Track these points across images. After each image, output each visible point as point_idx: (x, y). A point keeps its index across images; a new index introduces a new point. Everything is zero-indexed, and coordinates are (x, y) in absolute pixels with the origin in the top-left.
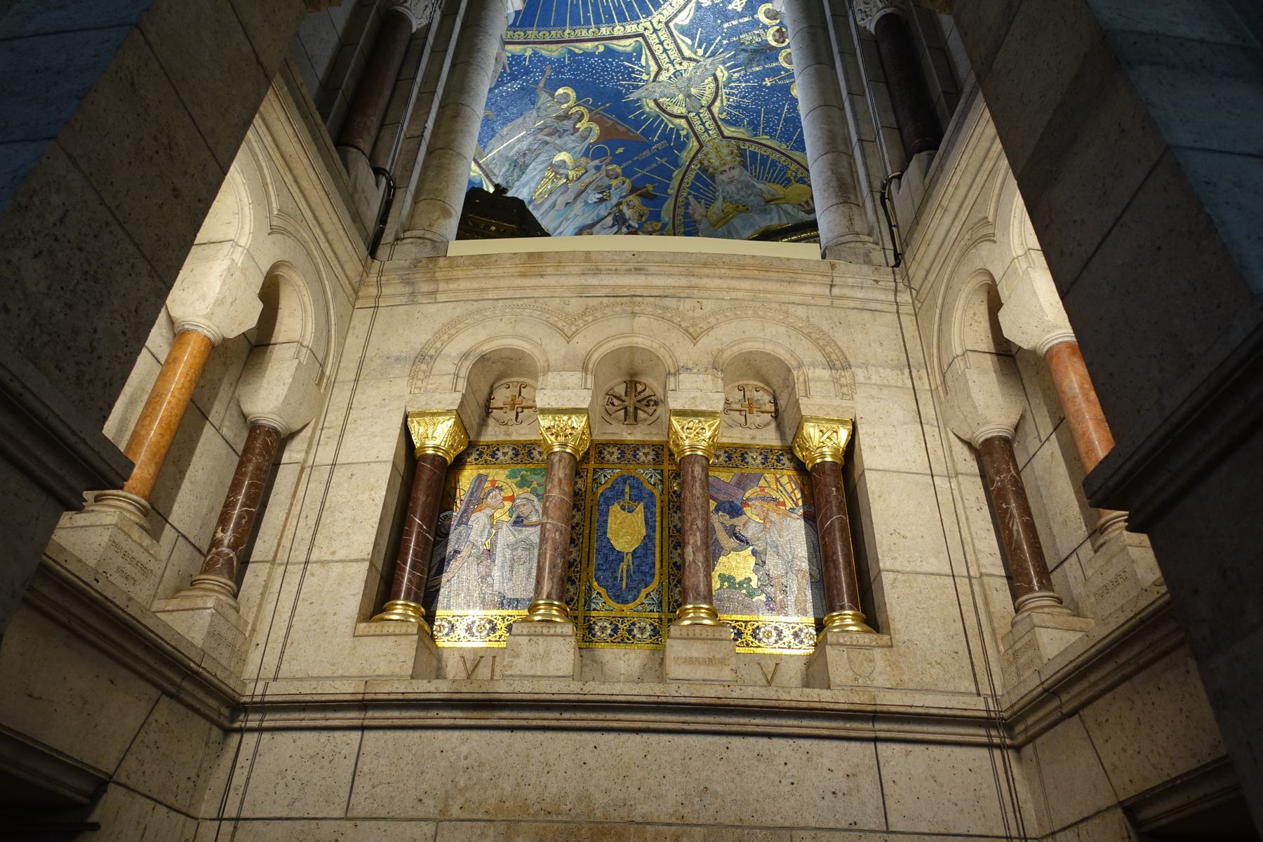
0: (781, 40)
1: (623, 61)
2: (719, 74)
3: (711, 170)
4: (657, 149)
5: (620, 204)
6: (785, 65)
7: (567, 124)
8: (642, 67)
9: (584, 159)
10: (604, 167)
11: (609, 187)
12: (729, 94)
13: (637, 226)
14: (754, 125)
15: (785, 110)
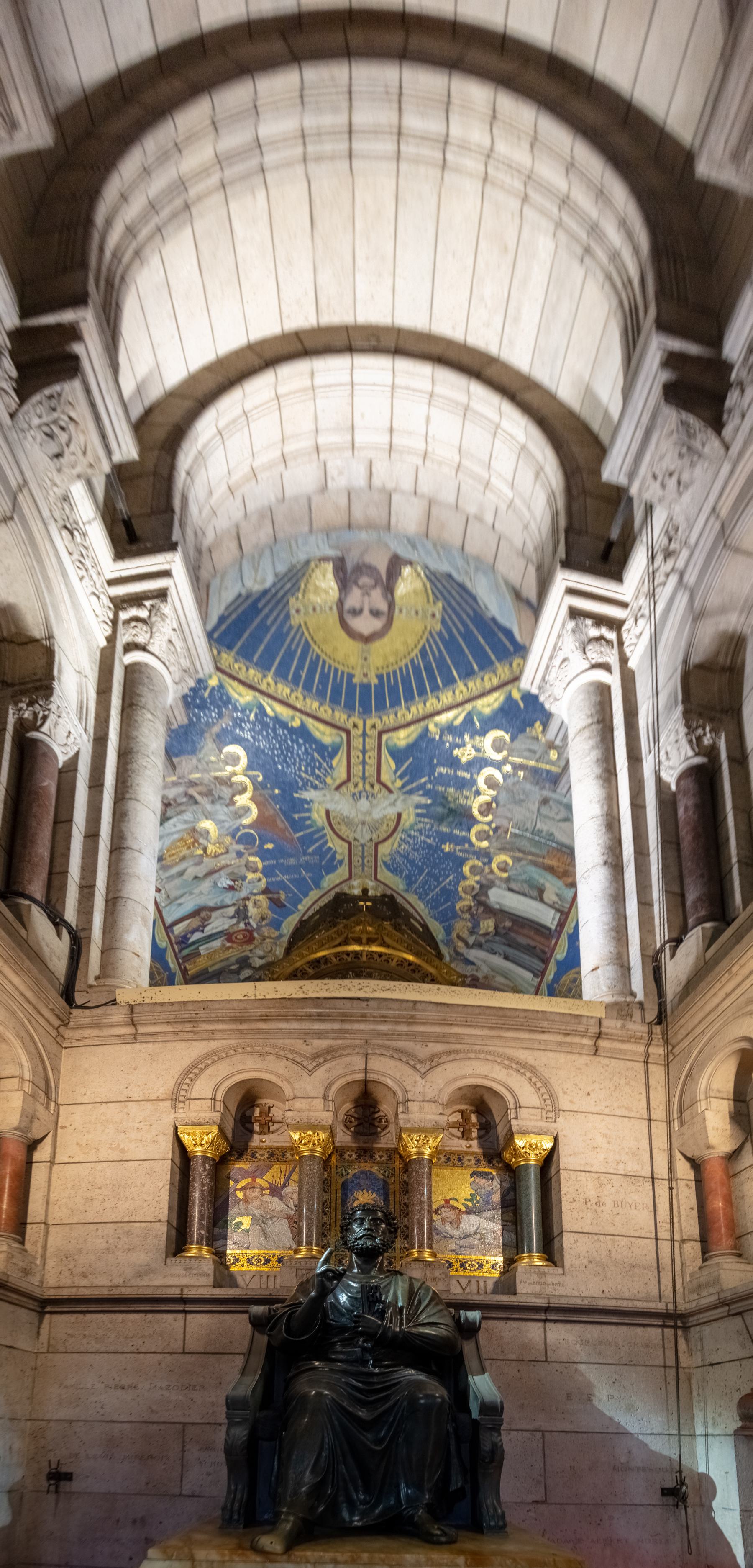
6: (473, 839)
7: (226, 792)
9: (229, 838)
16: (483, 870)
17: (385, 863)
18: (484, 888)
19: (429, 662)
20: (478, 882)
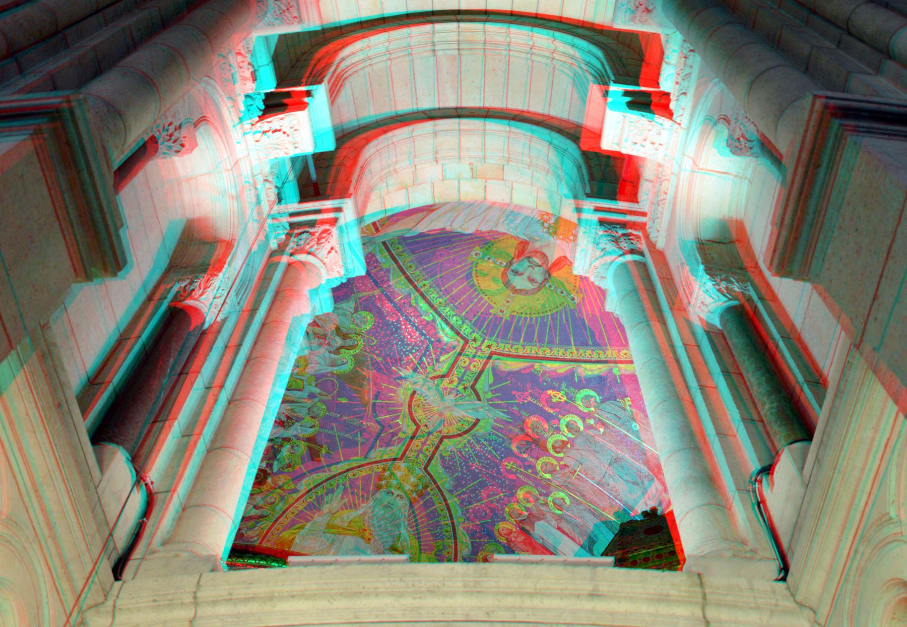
0: (558, 450)
1: (432, 342)
2: (481, 424)
3: (383, 482)
4: (368, 427)
5: (288, 440)
6: (539, 468)
8: (438, 361)
9: (314, 378)
10: (316, 400)
11: (299, 419)
12: (471, 444)
13: (275, 470)
14: (458, 483)
15: (497, 497)
16: (537, 499)
17: (442, 457)
18: (532, 518)
19: (555, 324)
20: (527, 509)
